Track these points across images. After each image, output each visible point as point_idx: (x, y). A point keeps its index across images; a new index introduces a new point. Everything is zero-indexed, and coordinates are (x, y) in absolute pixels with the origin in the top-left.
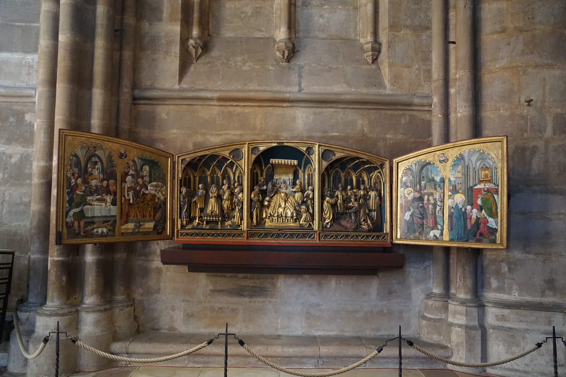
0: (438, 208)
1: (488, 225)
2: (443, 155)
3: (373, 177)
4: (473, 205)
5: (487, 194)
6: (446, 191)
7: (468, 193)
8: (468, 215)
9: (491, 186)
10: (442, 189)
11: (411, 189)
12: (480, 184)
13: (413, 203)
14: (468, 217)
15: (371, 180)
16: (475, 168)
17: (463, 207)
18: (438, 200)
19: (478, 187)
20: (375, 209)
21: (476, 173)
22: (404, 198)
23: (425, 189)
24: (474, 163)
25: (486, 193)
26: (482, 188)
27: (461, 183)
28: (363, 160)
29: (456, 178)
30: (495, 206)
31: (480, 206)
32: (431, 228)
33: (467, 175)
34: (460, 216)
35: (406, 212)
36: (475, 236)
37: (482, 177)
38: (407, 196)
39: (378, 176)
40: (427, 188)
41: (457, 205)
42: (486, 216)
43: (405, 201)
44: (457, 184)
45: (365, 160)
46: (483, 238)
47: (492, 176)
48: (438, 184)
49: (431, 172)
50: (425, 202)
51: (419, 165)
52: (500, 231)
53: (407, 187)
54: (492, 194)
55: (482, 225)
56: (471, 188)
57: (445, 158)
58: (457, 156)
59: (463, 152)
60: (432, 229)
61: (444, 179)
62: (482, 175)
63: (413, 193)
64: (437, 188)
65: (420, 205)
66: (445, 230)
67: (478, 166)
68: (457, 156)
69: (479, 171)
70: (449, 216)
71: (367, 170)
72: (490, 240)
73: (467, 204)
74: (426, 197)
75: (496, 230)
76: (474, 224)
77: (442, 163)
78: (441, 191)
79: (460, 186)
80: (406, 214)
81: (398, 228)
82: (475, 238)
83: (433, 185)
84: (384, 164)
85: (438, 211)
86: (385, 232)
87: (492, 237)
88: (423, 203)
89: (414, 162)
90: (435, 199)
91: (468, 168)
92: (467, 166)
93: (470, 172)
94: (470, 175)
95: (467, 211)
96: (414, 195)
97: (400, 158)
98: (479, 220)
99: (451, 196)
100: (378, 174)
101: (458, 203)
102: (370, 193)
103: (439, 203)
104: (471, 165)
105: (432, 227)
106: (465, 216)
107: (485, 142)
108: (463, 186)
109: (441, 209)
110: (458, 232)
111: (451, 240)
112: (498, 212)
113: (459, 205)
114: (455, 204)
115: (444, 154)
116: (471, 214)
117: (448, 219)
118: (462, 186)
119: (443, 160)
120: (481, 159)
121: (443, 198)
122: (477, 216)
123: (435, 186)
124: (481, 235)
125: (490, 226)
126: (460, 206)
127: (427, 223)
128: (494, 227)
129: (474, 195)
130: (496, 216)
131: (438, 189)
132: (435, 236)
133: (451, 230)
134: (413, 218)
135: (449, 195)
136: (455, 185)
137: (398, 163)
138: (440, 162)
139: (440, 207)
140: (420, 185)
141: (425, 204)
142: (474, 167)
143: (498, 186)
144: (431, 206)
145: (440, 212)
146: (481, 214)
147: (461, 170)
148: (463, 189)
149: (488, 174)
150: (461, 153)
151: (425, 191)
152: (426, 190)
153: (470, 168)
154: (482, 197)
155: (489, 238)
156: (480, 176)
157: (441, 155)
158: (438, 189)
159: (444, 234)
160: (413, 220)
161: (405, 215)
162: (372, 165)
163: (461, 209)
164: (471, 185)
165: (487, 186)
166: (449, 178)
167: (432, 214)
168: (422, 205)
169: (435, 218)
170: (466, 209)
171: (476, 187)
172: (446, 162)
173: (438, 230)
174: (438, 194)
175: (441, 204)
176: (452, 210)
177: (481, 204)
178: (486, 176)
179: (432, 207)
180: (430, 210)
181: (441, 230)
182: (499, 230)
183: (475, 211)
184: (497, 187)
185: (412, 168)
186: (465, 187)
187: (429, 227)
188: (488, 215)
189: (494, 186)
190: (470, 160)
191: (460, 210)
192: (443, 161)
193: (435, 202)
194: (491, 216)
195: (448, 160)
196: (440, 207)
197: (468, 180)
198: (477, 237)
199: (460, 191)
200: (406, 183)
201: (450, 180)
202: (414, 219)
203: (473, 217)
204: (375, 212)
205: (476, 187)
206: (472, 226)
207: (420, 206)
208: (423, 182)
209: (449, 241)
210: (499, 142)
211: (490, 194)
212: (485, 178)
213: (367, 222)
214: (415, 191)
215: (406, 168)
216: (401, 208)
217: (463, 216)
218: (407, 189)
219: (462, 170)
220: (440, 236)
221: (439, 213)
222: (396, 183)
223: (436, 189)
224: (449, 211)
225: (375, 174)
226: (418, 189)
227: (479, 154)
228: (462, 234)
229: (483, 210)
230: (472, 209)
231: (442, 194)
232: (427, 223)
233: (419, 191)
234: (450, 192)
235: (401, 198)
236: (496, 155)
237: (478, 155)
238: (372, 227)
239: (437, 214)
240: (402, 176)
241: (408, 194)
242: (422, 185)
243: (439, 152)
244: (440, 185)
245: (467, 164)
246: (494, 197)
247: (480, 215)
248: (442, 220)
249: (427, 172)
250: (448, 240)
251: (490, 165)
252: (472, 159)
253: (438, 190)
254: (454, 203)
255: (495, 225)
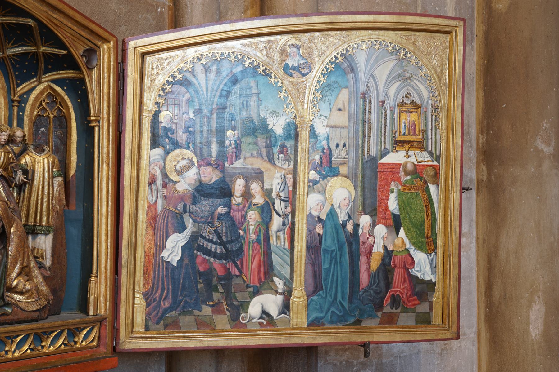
0: (277, 221)
1: (414, 272)
2: (295, 49)
3: (31, 101)
4: (375, 215)
5: (413, 183)
6: (301, 168)
7: (363, 177)
8: (363, 243)
9: (423, 157)
10: (289, 160)
11: (189, 154)
12: (396, 151)
13: (195, 201)
14: (363, 248)
15: (22, 109)
16: (383, 102)
17: (350, 218)
18: (278, 195)
19: (391, 158)
20: (52, 222)
21: (385, 118)
22: (165, 186)
23: (238, 157)
24: (381, 87)
25: (409, 177)
26: (400, 164)
27: (344, 145)
28: (22, 20)
29: (333, 127)
30: (430, 217)
31: (394, 215)
32: (251, 289)
33: (364, 121)
34: (341, 247)
35: (167, 237)
36: (379, 307)
37: (403, 131)
38: (174, 177)
39: (53, 96)
40: (243, 153)
41: (332, 214)
42: (408, 247)
43: (165, 197)
44: (333, 146)
45: (31, 22)
46: (399, 311)
47: (424, 131)
48: (279, 143)
49: (260, 101)
50: (237, 199)
51: (218, 72)
52: (441, 290)
53: (176, 145)
54: (426, 182)
55: (398, 274)
56: (374, 160)
57: (302, 62)
58: (336, 58)
59: (353, 48)
60: (257, 293)
61: (297, 127)
62: (403, 125)
63: (194, 170)
64: (276, 156)
65: (221, 210)
66: (295, 293)
67: (392, 97)
68: (336, 58)
69: (393, 113)
70: (308, 248)
71: (14, 66)
72: (418, 315)
73: (360, 208)
74: (239, 186)
75: (431, 285)
76: (379, 269)
77: (291, 75)
78: (285, 166)
79: (344, 152)
80: (170, 243)
81: (137, 295)
82: (379, 314)
83: (262, 142)
84: (95, 52)
85: (278, 231)
86: (91, 313)
87: (423, 308)
88: (228, 205)
89: (204, 61)
90: (267, 193)
91: (365, 101)
92: (364, 94)
93: (370, 112)
94: (370, 122)
95: (360, 232)
96: (199, 173)
97: (155, 39)
98: (390, 259)
99: (316, 182)
100: (58, 88)
101: (336, 206)
102: (26, 159)
103: (278, 205)
104: (373, 92)
105: (257, 284)
106: (354, 247)
107: (414, 27)
108: (352, 154)
109: (284, 224)
110: (336, 297)
111: (314, 324)
112: (436, 234)
113: (338, 211)
114: (327, 209)
115: (298, 47)
116: (371, 240)
117: (307, 257)
118: (348, 154)
119: (296, 65)
120: (399, 76)
121: (291, 188)
122: (385, 247)
123: (269, 147)
124: (396, 301)
125: (419, 275)
126: (342, 217)
127: (240, 271)
128: (427, 278)
129: (379, 183)
130: (432, 247)
131: (279, 160)
132: (265, 313)
133: (315, 292)
134: (193, 257)
135: (309, 181)
136: (329, 149)
137: (144, 55)
138: (286, 69)
139: (281, 220)
140: (221, 143)
141: (234, 207)
142: (382, 98)
143: (438, 159)
144: (253, 216)
145: (281, 234)
146: (396, 241)
147: (346, 104)
148: (351, 163)
149: (416, 123)
150: (347, 51)
151: (238, 164)
152: (242, 160)
153: (370, 102)
154: (399, 191)
155: (414, 311)
156: (397, 128)
157: (289, 50)
158: (279, 160)
159: (293, 307)
160: (193, 264)
161: (164, 247)
162: (42, 49)
163: (344, 225)
164: (371, 153)
165: (413, 159)
166: (312, 127)
167: (258, 241)
168: (226, 209)
169: (268, 252)
170: (356, 226)
171: (384, 160)
172: (304, 75)
173: (277, 292)
174: (278, 175)
175: (286, 207)
176: (319, 229)
177: (396, 212)
178: (412, 127)
179: (259, 219)
180: (252, 228)
181: (283, 294)
182: (439, 287)
183: (381, 230)
184: (435, 163)
185: (194, 80)
186: (357, 157)
187: (248, 287)
188: (414, 244)
189: (430, 159)
190: (372, 76)
191: (341, 230)
192: (297, 69)
193: (266, 203)
194: (420, 248)
195: (310, 67)
196: (281, 220)
197: (364, 137)
198: (385, 311)
199: (343, 170)
200: (170, 129)
201: (313, 134)
202: (198, 260)
203: (375, 250)
204: (50, 237)
205: (384, 160)
206: (372, 277)
207: (220, 215)
208: (229, 133)
209: (308, 326)
210: (444, 35)
211: (420, 183)
212: (409, 134)
213: (30, 279)
214: (205, 161)
215: (174, 77)
216: (153, 219)
217: (350, 245)
218: (177, 151)
219: (350, 103)
220: (280, 314)
221: (278, 237)
222: (137, 130)
223: (271, 160)
224: (310, 231)
225: (42, 87)
226: (214, 154)
227: (395, 62)
228: (346, 304)
229: (402, 229)
230: (374, 225)
231: (290, 177)
232: (240, 271)
233: (219, 165)
234: (313, 172)
235: (150, 184)
236: (436, 71)
237: (392, 64)
238: (51, 297)
239: (273, 241)
240: (157, 103)
241: (180, 172)
242: (227, 142)
243: (285, 37)
244: (283, 146)
245: (362, 89)
246: (427, 190)
247: (394, 245)
248: (288, 260)
249: (246, 99)
250: (305, 325)
251: (420, 97)
252: (376, 73)
253: (279, 163)
254: (323, 205)
255: (430, 273)
